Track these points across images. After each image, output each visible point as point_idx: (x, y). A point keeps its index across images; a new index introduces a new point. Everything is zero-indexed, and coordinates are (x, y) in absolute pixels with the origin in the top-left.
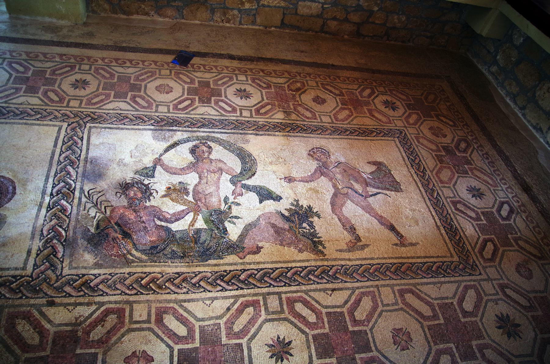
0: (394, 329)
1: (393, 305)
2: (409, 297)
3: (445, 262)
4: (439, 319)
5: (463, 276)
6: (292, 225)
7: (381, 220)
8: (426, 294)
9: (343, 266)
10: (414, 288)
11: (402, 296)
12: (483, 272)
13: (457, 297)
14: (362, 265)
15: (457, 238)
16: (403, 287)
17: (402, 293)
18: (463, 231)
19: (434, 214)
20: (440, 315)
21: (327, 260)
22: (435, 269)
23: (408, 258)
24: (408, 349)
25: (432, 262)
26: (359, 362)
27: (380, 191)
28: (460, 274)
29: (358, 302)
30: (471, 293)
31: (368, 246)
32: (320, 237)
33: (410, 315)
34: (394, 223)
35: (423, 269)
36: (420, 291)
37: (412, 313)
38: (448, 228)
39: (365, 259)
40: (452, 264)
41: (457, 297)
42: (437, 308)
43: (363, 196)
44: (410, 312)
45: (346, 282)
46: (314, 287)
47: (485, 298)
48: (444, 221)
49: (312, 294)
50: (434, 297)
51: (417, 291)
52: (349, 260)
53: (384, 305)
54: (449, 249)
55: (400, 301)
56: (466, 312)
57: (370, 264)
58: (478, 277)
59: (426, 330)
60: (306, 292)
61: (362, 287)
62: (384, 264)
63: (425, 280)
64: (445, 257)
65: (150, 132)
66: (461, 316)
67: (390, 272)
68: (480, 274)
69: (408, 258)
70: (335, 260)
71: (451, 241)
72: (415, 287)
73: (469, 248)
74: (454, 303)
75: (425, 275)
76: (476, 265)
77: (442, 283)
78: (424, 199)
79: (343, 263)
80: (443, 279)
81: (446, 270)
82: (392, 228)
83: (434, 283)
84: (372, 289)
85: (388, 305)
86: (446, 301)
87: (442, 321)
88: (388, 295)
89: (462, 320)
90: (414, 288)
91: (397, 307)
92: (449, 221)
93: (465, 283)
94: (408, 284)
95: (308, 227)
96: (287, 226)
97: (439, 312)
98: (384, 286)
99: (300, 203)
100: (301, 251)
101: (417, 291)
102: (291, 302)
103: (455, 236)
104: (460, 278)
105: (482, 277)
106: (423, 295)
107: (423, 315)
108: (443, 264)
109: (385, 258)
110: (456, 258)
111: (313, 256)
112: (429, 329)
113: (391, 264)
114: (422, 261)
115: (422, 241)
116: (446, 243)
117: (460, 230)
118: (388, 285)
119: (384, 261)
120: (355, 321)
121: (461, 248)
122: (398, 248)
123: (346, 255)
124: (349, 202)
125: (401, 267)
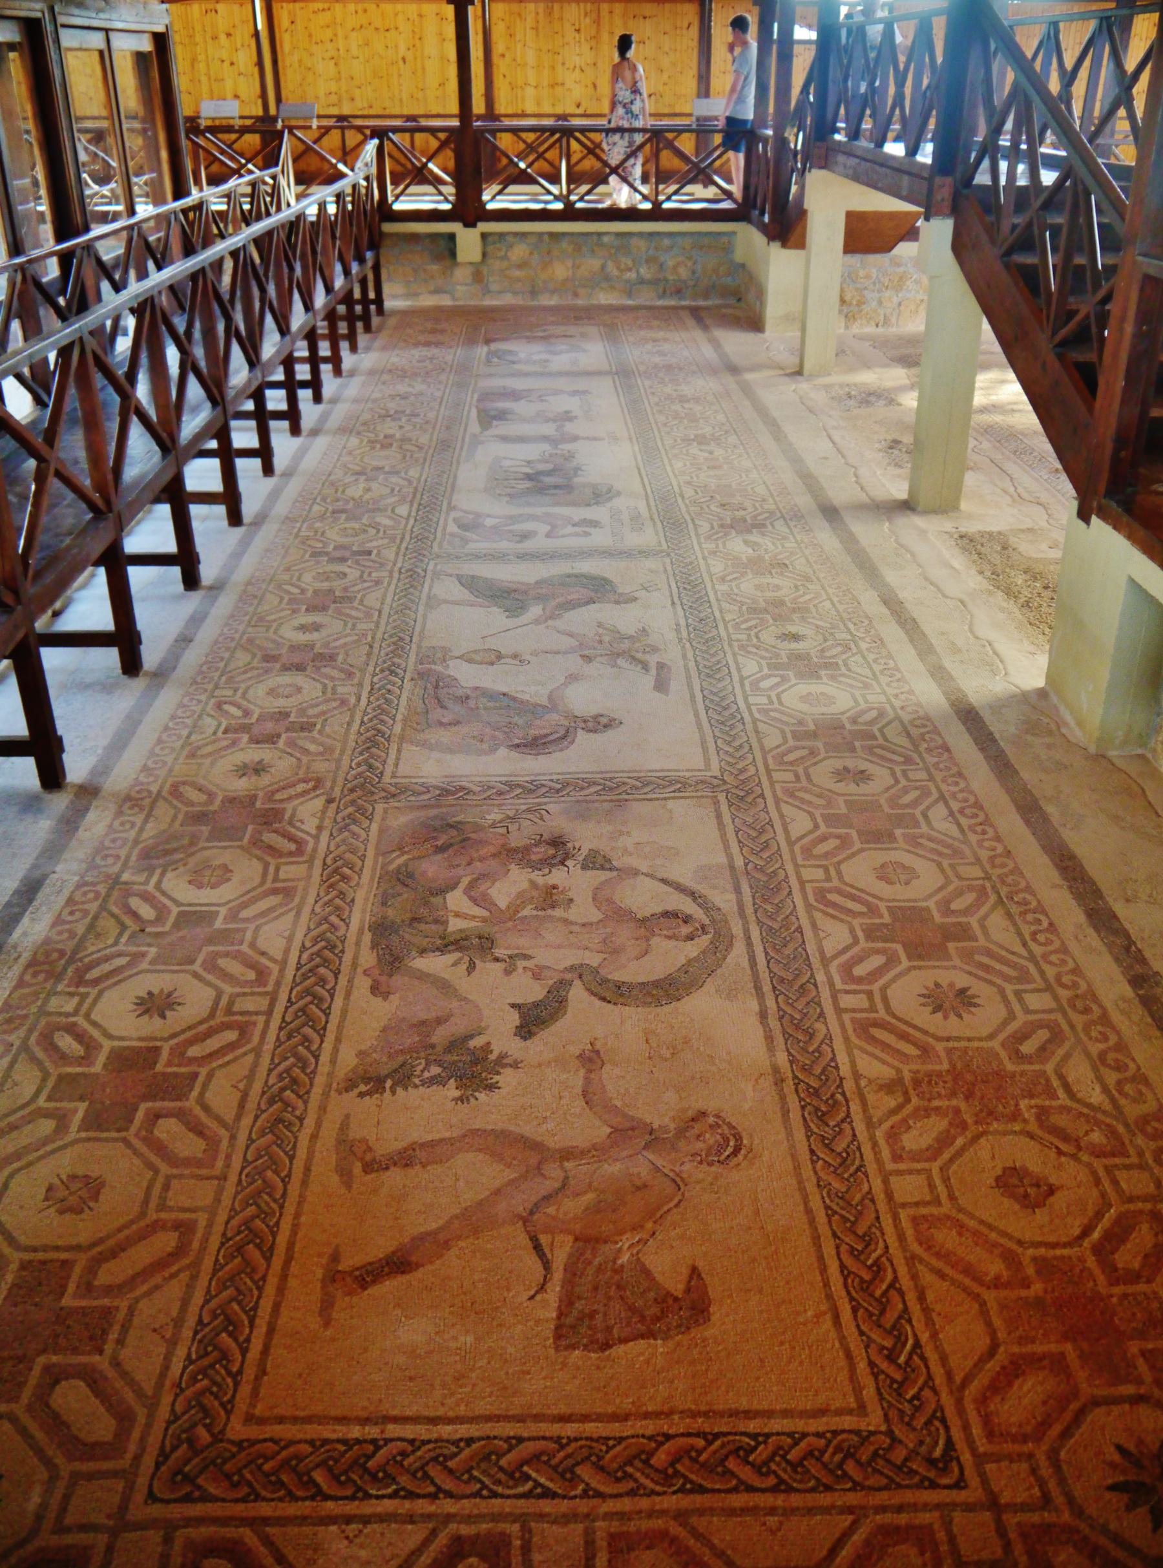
0: (103, 1184)
1: (163, 1198)
2: (167, 1241)
3: (236, 1384)
4: (75, 1296)
5: (169, 1423)
6: (439, 1049)
7: (438, 1243)
8: (157, 1287)
9: (301, 1119)
10: (186, 1261)
11: (178, 1226)
12: (156, 1510)
13: (111, 1373)
14: (292, 1158)
15: (318, 1476)
16: (199, 1235)
17: (184, 1228)
18: (349, 1519)
19: (446, 1431)
20: (84, 1303)
21: (326, 1095)
22: (221, 1343)
23: (284, 1277)
24: (46, 1199)
25: (248, 1340)
26: (72, 1105)
27: (558, 1275)
28: (177, 1418)
29: (198, 1130)
30: (103, 1428)
31: (348, 1184)
32: (394, 1093)
33: (120, 1230)
34: (419, 1274)
35: (235, 1306)
36: (173, 1276)
37: (121, 1236)
38: (369, 1457)
39: (307, 1170)
40: (223, 1405)
41: (111, 1373)
42: (106, 1302)
43: (532, 1213)
44: (126, 1232)
45: (257, 1117)
46: (266, 1061)
47: (66, 1468)
48: (404, 1454)
49: (250, 1058)
50: (140, 1305)
51: (174, 1268)
52: (314, 1137)
53: (169, 1178)
54: (281, 1420)
55: (163, 1215)
56: (57, 1382)
57: (289, 1175)
58: (142, 1482)
59: (64, 1256)
60: (257, 1052)
61: (232, 1145)
62: (282, 1207)
63: (198, 1298)
64: (255, 1394)
65: (722, 859)
66: (54, 1359)
67: (253, 1217)
68: (151, 1497)
69: (284, 1277)
70: (323, 1109)
71: (311, 1442)
72: (188, 1267)
73: (265, 1509)
74: (97, 1358)
75: (213, 1304)
76: (187, 1499)
77: (173, 1343)
78: (521, 1419)
79: (310, 1121)
80: (181, 1352)
81: (206, 1376)
82: (398, 1264)
83: (178, 1322)
84: (220, 1164)
85: (166, 1187)
86: (113, 1336)
87: (67, 1301)
88: (192, 1195)
89: (42, 1360)
90: (186, 1261)
91: (153, 1204)
92: (404, 1480)
93: (141, 1419)
94: (203, 1248)
95: (426, 1074)
96: (434, 1039)
97: (96, 1303)
98: (220, 1191)
99: (508, 1071)
100: (361, 1054)
101: (174, 1268)
102: (244, 1030)
103: (330, 1470)
104: (164, 1412)
105: (139, 1496)
106: (157, 1279)
107: (107, 1260)
108: (229, 1373)
109: (297, 1215)
110: (237, 1429)
111: (341, 1072)
112: (64, 1262)
113: (277, 1224)
114: (260, 1312)
115: (333, 1339)
116: (309, 1420)
117: (351, 1508)
118: (218, 1200)
119: (290, 1209)
120: (158, 1116)
121: (276, 1471)
122: (324, 1261)
123: (329, 1133)
124: (510, 1174)
125: (259, 1247)
